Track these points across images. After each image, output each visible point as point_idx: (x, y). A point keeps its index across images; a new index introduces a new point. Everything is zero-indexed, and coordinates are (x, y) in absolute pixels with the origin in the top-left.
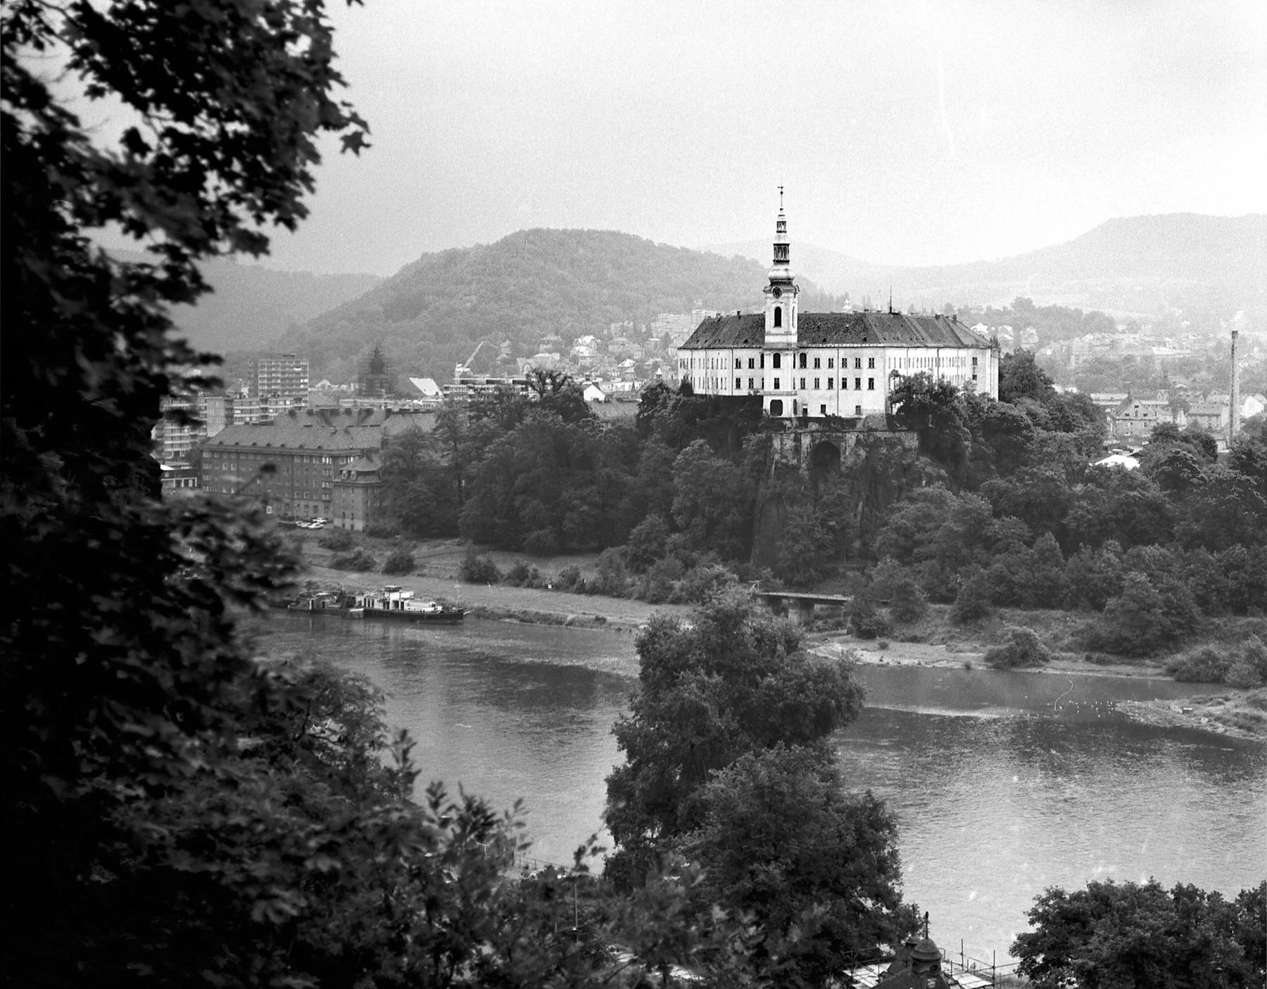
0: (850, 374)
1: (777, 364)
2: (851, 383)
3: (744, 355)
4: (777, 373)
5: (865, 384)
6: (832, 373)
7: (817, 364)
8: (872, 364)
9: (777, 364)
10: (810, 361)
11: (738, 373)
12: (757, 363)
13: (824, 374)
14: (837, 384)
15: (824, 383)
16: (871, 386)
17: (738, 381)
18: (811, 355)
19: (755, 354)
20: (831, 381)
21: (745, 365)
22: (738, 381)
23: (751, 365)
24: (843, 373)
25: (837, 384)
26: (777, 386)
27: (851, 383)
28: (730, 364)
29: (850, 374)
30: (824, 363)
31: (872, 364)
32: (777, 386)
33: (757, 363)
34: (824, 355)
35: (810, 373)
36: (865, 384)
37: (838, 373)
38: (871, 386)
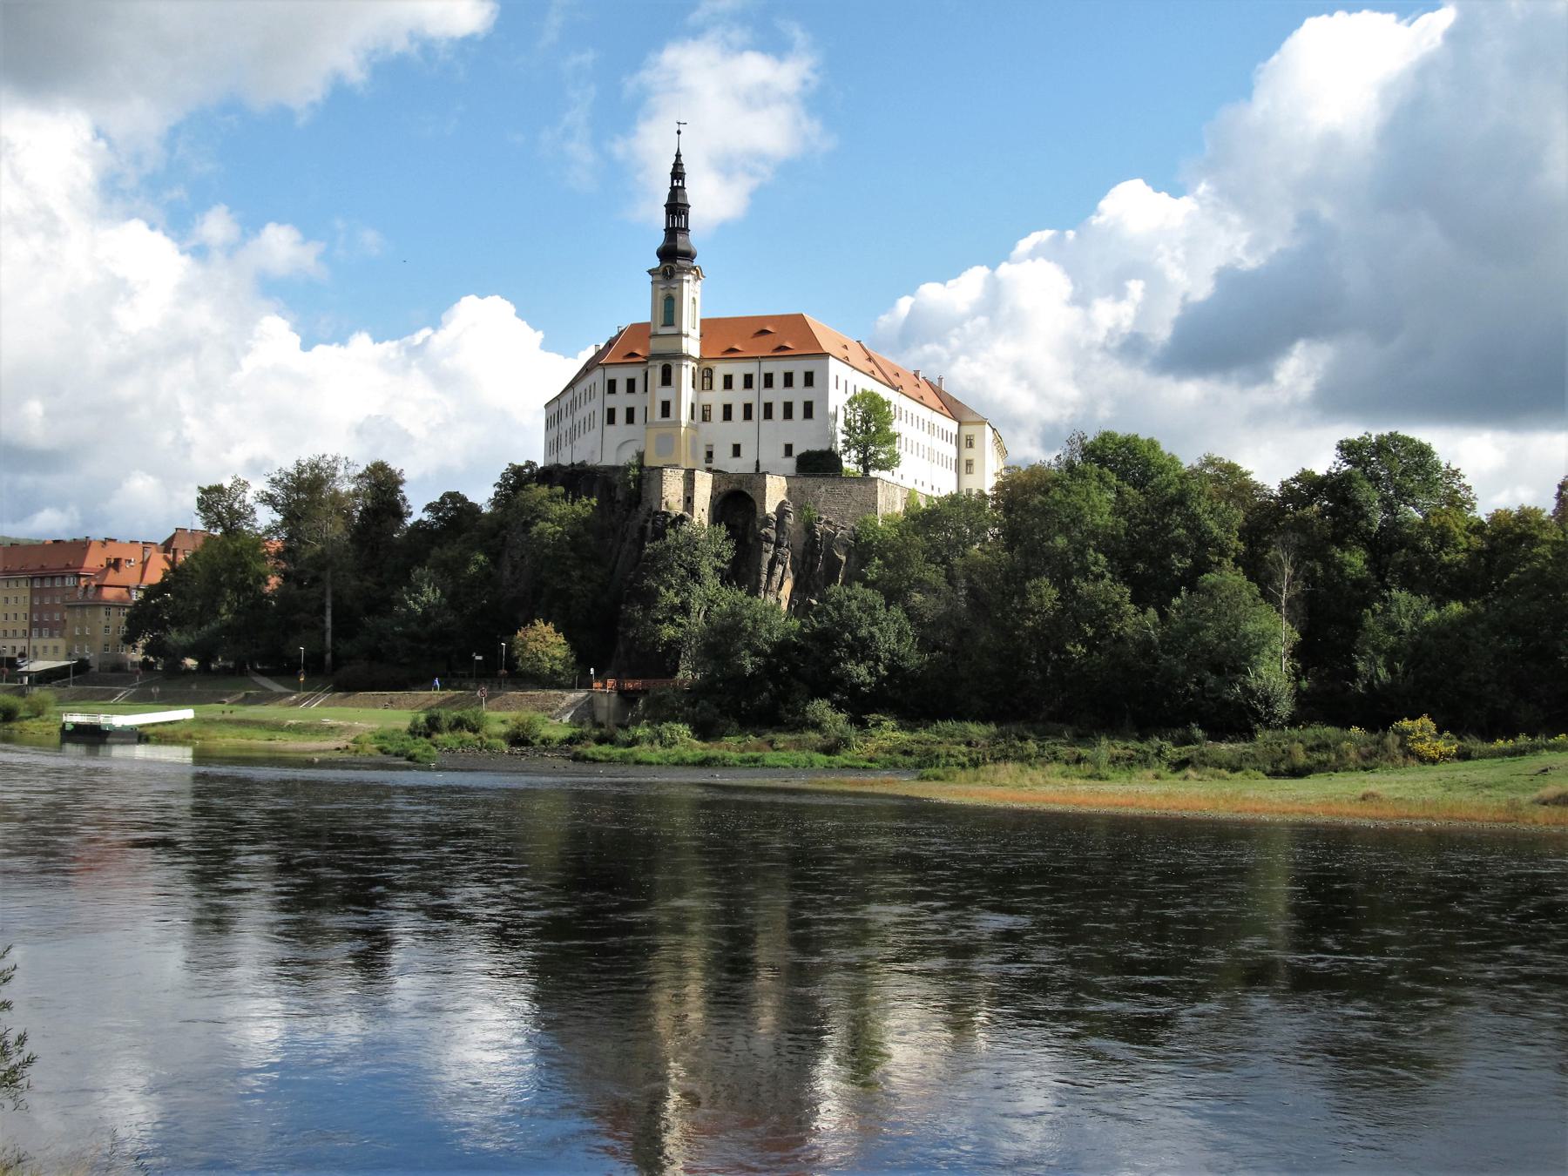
0: (778, 396)
1: (666, 380)
2: (778, 411)
4: (665, 393)
5: (798, 410)
6: (750, 396)
8: (809, 379)
10: (718, 381)
11: (611, 401)
12: (639, 385)
13: (738, 396)
14: (758, 411)
15: (738, 412)
17: (611, 415)
18: (720, 370)
20: (748, 409)
21: (621, 386)
25: (758, 411)
27: (778, 411)
28: (601, 387)
29: (778, 396)
30: (738, 382)
34: (738, 370)
35: (717, 397)
36: (798, 410)
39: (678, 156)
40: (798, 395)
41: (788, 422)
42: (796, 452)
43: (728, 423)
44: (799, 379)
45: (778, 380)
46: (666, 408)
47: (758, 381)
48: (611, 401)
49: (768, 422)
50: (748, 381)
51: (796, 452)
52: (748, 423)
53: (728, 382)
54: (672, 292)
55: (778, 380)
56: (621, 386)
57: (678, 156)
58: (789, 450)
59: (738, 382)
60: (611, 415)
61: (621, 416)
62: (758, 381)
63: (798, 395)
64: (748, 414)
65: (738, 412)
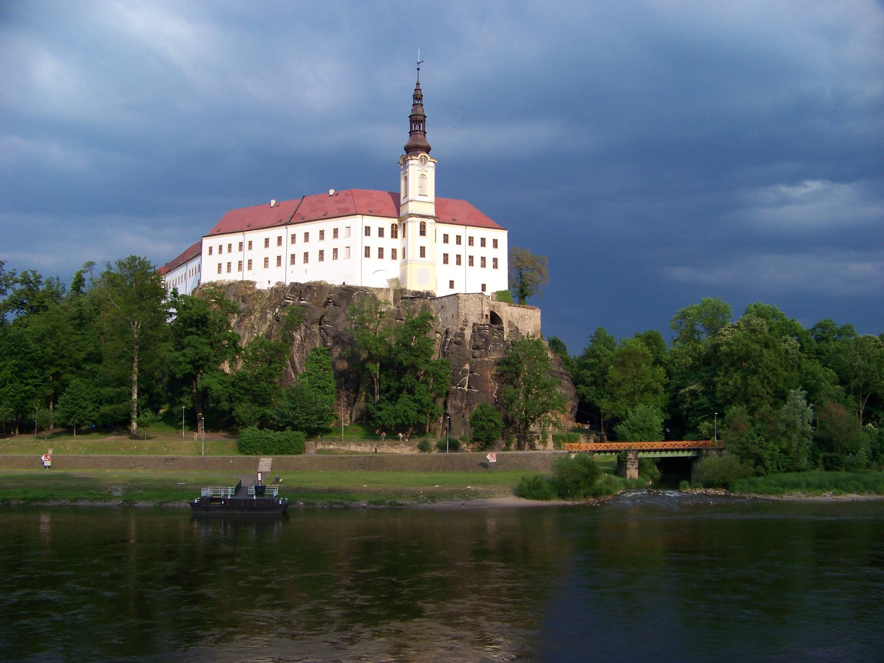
0: (477, 251)
1: (423, 233)
3: (375, 223)
5: (489, 263)
8: (495, 243)
9: (423, 233)
14: (465, 260)
16: (495, 266)
17: (367, 249)
19: (387, 223)
21: (374, 232)
22: (367, 249)
23: (381, 232)
25: (465, 260)
29: (477, 251)
31: (495, 243)
33: (388, 232)
34: (453, 231)
36: (489, 263)
37: (464, 250)
38: (495, 266)
39: (418, 84)
40: (489, 252)
46: (423, 249)
47: (465, 240)
54: (425, 173)
56: (374, 232)
57: (418, 84)
61: (374, 252)
62: (465, 240)
63: (489, 252)
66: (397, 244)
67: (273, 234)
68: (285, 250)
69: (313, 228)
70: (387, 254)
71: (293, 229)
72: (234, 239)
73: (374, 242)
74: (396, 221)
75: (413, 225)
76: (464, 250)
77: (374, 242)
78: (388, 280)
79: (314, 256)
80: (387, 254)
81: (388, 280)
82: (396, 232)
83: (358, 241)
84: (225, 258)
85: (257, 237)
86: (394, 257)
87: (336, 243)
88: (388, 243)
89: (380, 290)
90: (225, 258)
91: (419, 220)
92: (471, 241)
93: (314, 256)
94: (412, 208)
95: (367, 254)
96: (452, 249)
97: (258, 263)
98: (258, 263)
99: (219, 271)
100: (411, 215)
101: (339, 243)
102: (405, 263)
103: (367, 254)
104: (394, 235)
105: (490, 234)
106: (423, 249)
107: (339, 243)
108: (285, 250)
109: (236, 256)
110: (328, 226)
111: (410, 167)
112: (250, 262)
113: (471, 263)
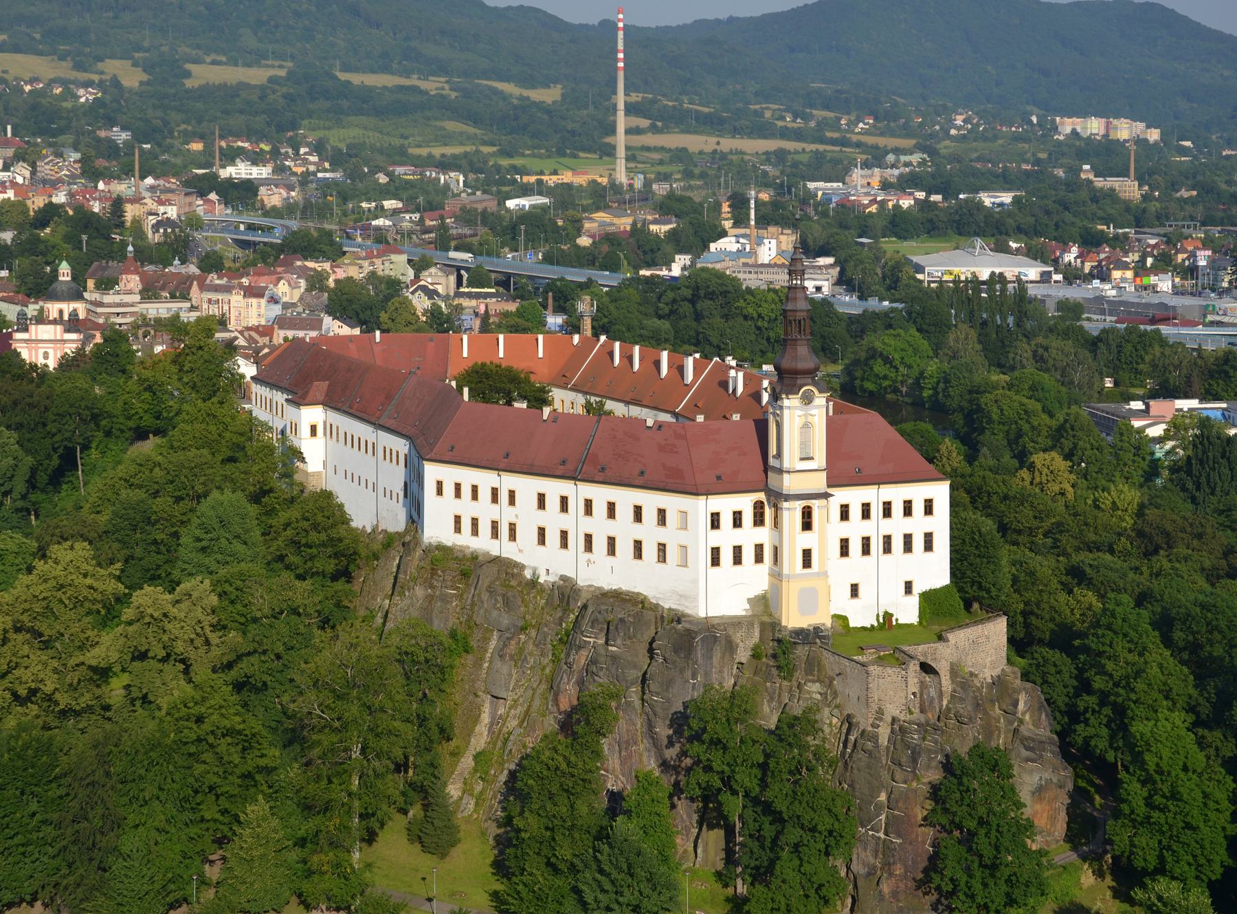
0: (897, 526)
1: (807, 526)
2: (897, 544)
3: (726, 504)
5: (918, 543)
7: (845, 513)
8: (929, 508)
9: (807, 526)
11: (715, 539)
14: (876, 545)
15: (855, 547)
16: (928, 546)
17: (716, 552)
19: (745, 503)
20: (866, 543)
21: (726, 520)
24: (887, 526)
25: (876, 545)
26: (807, 563)
27: (897, 544)
29: (897, 526)
30: (855, 512)
32: (807, 563)
33: (748, 518)
36: (918, 543)
37: (876, 528)
38: (928, 546)
40: (918, 525)
41: (908, 555)
42: (918, 589)
43: (845, 559)
44: (918, 508)
45: (897, 509)
46: (807, 554)
47: (877, 510)
48: (715, 539)
49: (888, 556)
50: (866, 512)
51: (918, 589)
52: (866, 558)
53: (845, 513)
55: (897, 509)
56: (726, 520)
58: (908, 587)
59: (855, 512)
60: (716, 552)
62: (877, 510)
63: (918, 525)
64: (866, 550)
65: (855, 547)
66: (763, 535)
67: (555, 488)
68: (577, 524)
69: (626, 498)
70: (748, 555)
71: (588, 490)
72: (486, 479)
73: (726, 538)
74: (761, 496)
75: (792, 514)
76: (876, 528)
77: (726, 538)
78: (749, 601)
79: (625, 548)
80: (748, 555)
81: (749, 601)
82: (762, 515)
83: (702, 539)
84: (466, 508)
85: (527, 486)
86: (759, 558)
87: (662, 534)
88: (750, 536)
89: (736, 622)
90: (466, 508)
91: (799, 505)
92: (887, 511)
93: (625, 548)
94: (790, 484)
95: (716, 561)
96: (856, 529)
97: (527, 534)
98: (527, 534)
99: (458, 529)
100: (788, 498)
101: (668, 535)
102: (777, 576)
103: (716, 561)
104: (759, 520)
105: (918, 492)
106: (807, 554)
107: (668, 535)
108: (577, 524)
109: (485, 511)
110: (651, 501)
111: (786, 412)
112: (512, 528)
113: (887, 549)
